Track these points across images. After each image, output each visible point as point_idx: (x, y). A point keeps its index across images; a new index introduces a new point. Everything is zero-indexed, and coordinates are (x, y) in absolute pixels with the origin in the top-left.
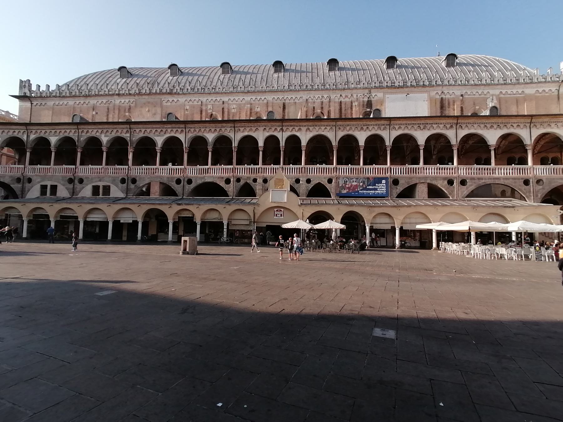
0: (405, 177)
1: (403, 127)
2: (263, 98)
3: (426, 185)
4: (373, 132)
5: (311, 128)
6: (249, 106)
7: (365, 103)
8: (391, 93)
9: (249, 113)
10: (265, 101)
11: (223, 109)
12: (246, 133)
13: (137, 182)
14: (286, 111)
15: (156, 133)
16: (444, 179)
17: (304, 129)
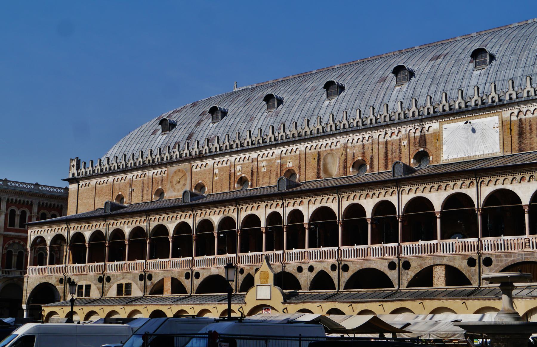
0: (417, 257)
1: (414, 188)
2: (295, 148)
3: (444, 267)
4: (382, 198)
5: (313, 199)
6: (279, 161)
7: (418, 140)
8: (450, 122)
9: (279, 172)
10: (298, 152)
11: (252, 169)
12: (249, 212)
13: (153, 279)
14: (322, 162)
15: (169, 220)
16: (464, 258)
17: (306, 200)
